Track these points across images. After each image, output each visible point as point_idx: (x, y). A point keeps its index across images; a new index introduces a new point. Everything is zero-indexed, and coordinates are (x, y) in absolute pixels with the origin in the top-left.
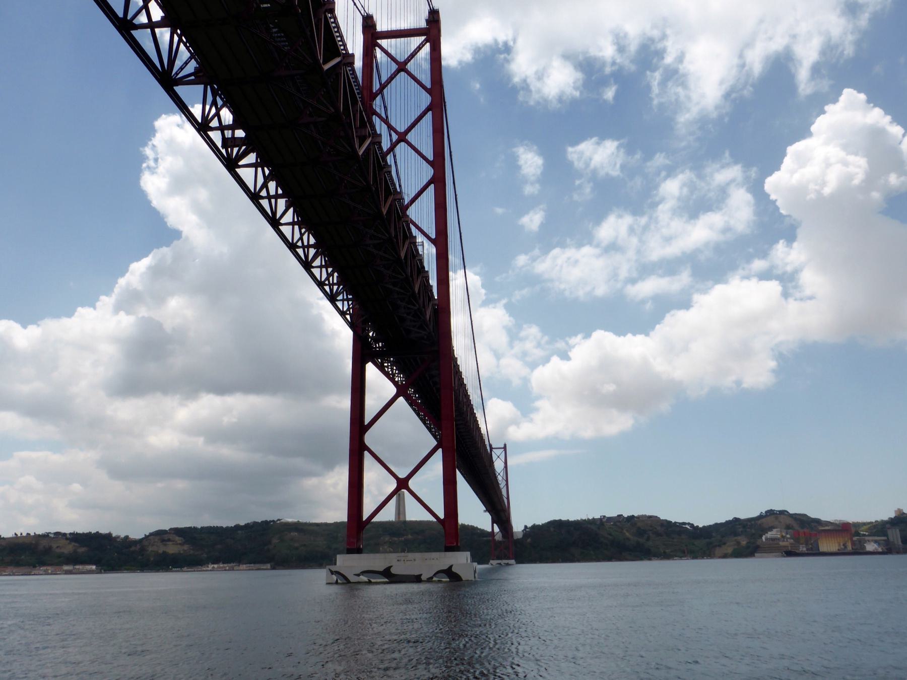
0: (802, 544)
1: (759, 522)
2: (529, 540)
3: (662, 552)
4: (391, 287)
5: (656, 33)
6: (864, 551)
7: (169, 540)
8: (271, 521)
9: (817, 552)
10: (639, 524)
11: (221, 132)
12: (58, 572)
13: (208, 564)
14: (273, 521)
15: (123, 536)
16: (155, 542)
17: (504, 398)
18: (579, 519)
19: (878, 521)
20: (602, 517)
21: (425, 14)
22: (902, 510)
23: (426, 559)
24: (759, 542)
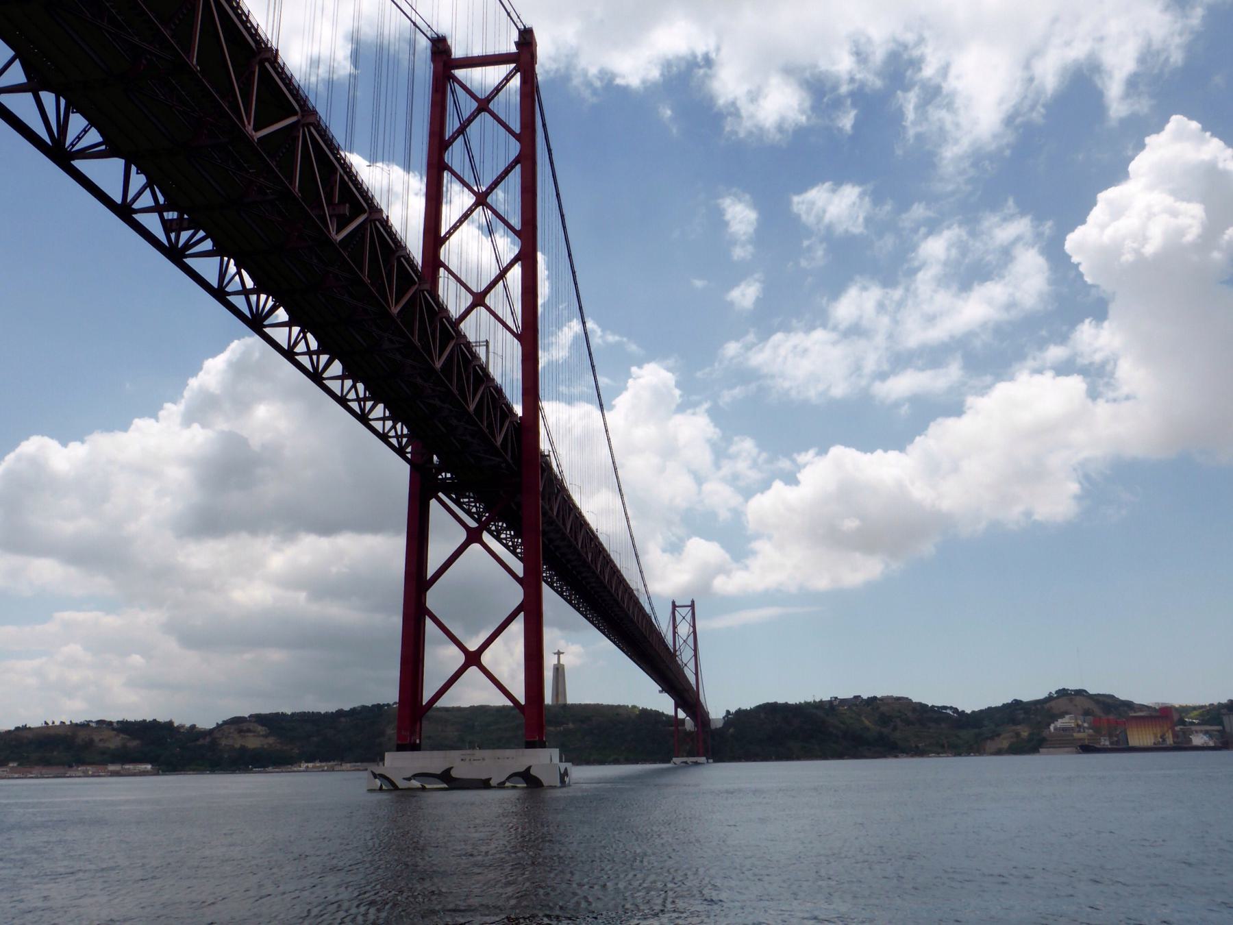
0: (1104, 736)
1: (1047, 706)
2: (731, 730)
3: (913, 745)
5: (910, 37)
6: (1190, 745)
7: (249, 731)
8: (384, 705)
9: (1124, 746)
10: (883, 709)
12: (101, 774)
13: (301, 762)
14: (388, 705)
15: (188, 725)
16: (230, 733)
17: (708, 536)
18: (803, 702)
20: (833, 699)
21: (515, 36)
24: (1045, 733)
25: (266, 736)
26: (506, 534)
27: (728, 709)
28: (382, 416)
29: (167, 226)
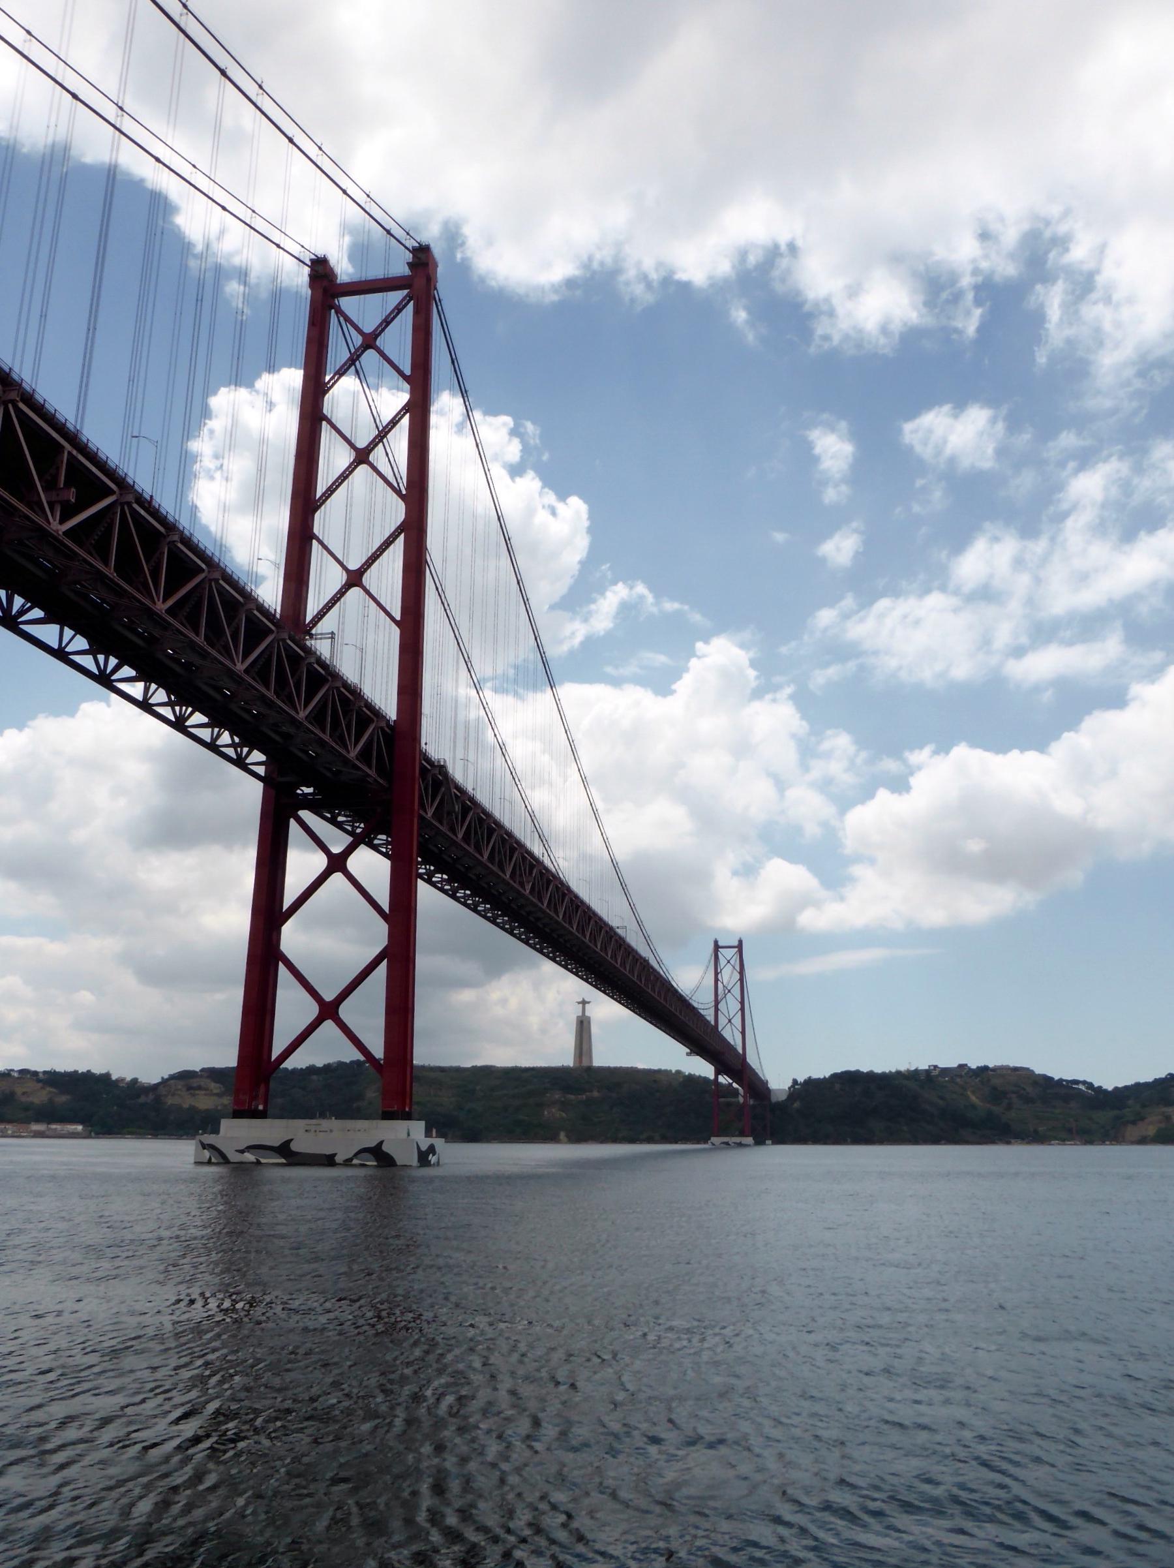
3: (1032, 1129)
5: (1055, 210)
7: (200, 1088)
10: (996, 1082)
15: (129, 1079)
25: (219, 1095)
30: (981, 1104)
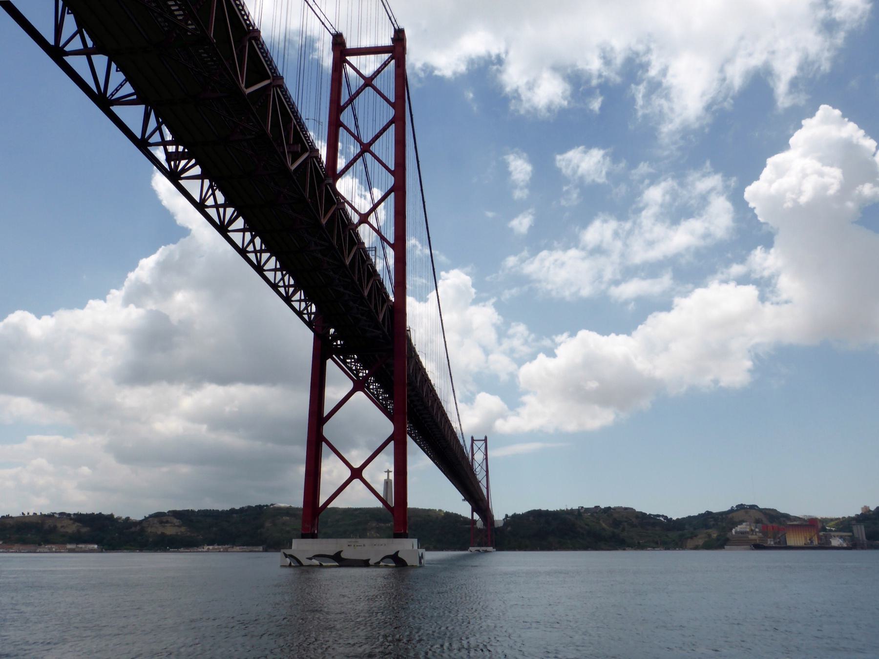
0: (770, 538)
1: (730, 516)
2: (509, 529)
3: (637, 542)
4: (342, 290)
5: (641, 48)
7: (167, 522)
8: (264, 506)
9: (785, 545)
11: (164, 148)
12: (62, 551)
13: (204, 545)
15: (124, 517)
16: (154, 524)
17: (492, 391)
18: (559, 510)
19: (845, 517)
20: (580, 508)
21: (392, 34)
22: (869, 507)
23: (375, 545)
24: (729, 535)
26: (373, 385)
27: (506, 513)
28: (299, 299)
29: (169, 156)
30: (608, 528)
